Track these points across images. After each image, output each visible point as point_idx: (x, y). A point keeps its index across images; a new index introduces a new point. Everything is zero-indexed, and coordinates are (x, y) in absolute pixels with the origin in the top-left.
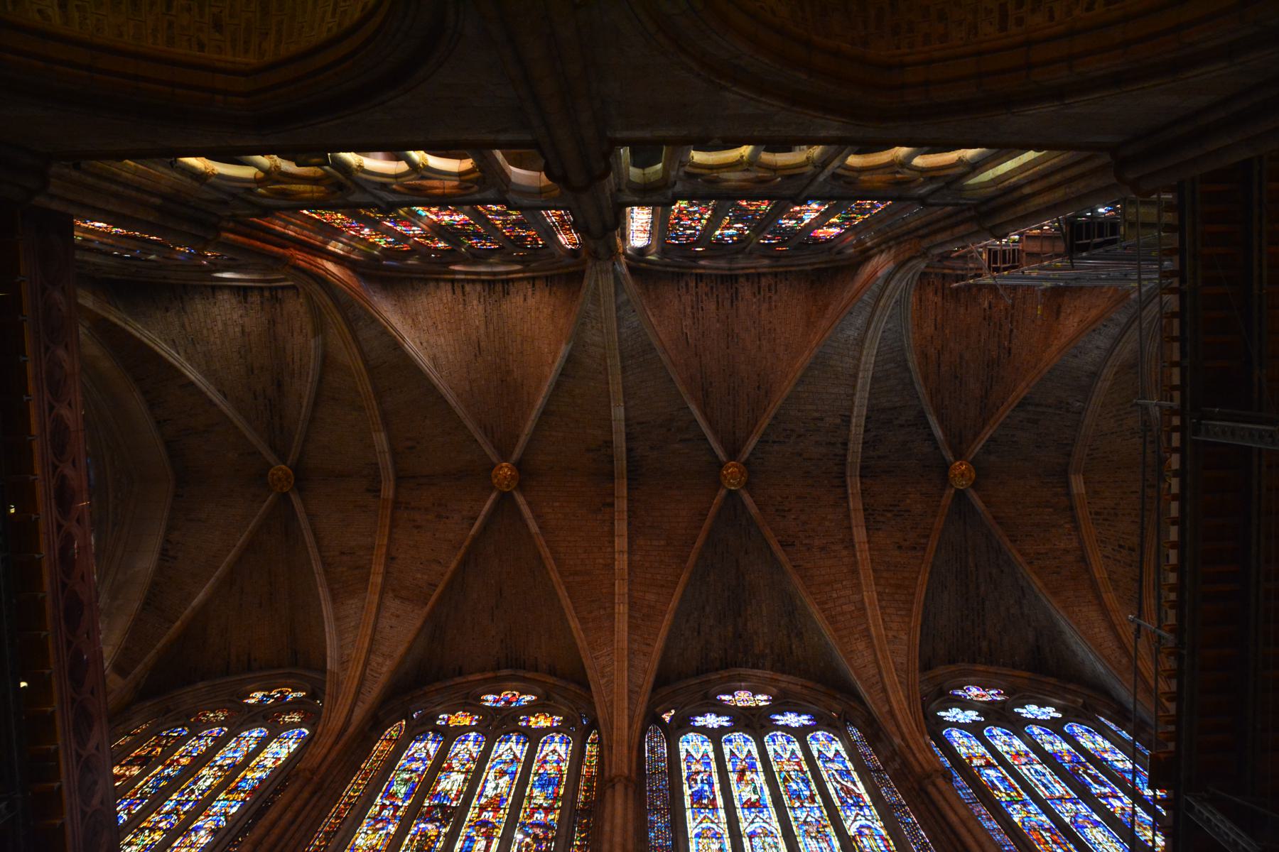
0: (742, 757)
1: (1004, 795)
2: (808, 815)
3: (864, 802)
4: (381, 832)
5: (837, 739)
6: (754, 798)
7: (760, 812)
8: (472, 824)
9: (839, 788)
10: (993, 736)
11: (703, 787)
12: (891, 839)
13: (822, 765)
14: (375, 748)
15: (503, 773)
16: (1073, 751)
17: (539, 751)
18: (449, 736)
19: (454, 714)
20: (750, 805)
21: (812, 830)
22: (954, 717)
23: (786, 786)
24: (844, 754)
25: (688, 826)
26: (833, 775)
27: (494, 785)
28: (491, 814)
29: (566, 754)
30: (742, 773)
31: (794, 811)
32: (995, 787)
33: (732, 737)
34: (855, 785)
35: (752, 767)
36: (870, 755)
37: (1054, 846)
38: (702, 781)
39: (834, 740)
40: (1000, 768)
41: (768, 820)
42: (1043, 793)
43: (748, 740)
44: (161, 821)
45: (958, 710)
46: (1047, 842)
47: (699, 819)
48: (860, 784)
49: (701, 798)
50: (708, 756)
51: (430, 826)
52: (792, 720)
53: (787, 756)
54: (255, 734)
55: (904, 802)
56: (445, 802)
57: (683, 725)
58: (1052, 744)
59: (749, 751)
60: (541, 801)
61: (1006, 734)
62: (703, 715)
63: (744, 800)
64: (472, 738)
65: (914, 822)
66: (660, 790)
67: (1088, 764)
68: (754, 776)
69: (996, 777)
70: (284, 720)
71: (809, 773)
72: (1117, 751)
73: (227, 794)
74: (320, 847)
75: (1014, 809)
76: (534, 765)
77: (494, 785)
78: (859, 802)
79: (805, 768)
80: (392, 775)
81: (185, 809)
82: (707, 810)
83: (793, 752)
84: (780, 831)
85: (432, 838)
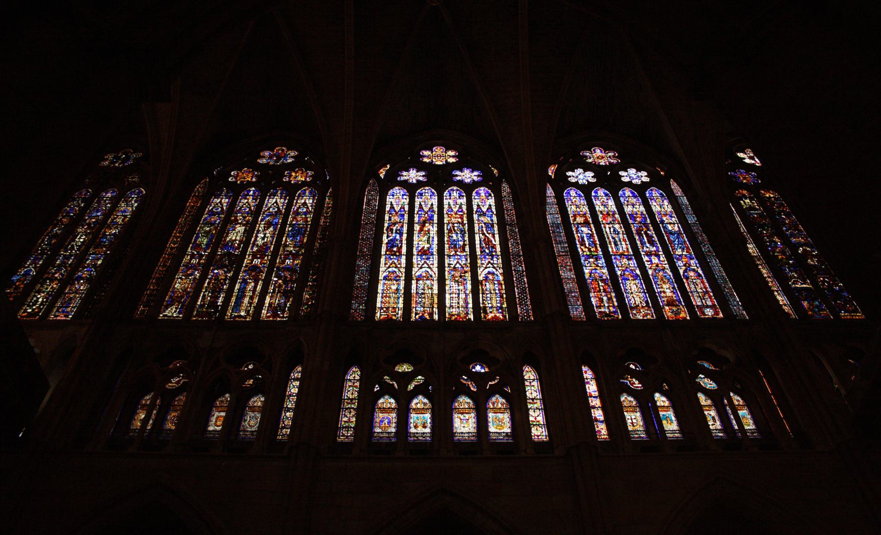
0: (426, 209)
1: (587, 250)
2: (458, 262)
3: (496, 252)
4: (190, 278)
5: (493, 195)
7: (428, 259)
8: (247, 269)
9: (482, 240)
10: (596, 197)
11: (396, 237)
12: (505, 284)
13: (477, 218)
14: (188, 204)
15: (269, 225)
16: (645, 213)
17: (294, 204)
18: (237, 191)
19: (241, 171)
20: (424, 253)
21: (457, 274)
22: (577, 177)
23: (449, 236)
24: (494, 210)
25: (381, 269)
26: (482, 227)
27: (263, 236)
28: (259, 260)
29: (311, 206)
30: (423, 225)
31: (450, 258)
32: (583, 243)
34: (494, 237)
35: (431, 218)
36: (511, 210)
37: (603, 294)
38: (396, 230)
39: (490, 195)
41: (431, 266)
42: (612, 249)
43: (433, 193)
44: (56, 273)
45: (581, 170)
46: (600, 291)
47: (389, 264)
48: (497, 236)
49: (393, 246)
50: (404, 208)
51: (221, 272)
52: (467, 176)
53: (455, 210)
54: (109, 195)
55: (521, 253)
56: (231, 251)
57: (392, 181)
58: (633, 205)
59: (432, 205)
60: (292, 249)
61: (606, 195)
62: (408, 171)
63: (420, 248)
64: (251, 193)
65: (522, 269)
67: (650, 225)
68: (431, 228)
69: (587, 234)
70: (128, 181)
71: (467, 225)
72: (674, 215)
73: (94, 249)
74: (153, 290)
75: (589, 262)
76: (290, 216)
77: (264, 236)
79: (465, 222)
80: (198, 229)
81: (69, 263)
82: (395, 257)
83: (460, 207)
85: (222, 281)
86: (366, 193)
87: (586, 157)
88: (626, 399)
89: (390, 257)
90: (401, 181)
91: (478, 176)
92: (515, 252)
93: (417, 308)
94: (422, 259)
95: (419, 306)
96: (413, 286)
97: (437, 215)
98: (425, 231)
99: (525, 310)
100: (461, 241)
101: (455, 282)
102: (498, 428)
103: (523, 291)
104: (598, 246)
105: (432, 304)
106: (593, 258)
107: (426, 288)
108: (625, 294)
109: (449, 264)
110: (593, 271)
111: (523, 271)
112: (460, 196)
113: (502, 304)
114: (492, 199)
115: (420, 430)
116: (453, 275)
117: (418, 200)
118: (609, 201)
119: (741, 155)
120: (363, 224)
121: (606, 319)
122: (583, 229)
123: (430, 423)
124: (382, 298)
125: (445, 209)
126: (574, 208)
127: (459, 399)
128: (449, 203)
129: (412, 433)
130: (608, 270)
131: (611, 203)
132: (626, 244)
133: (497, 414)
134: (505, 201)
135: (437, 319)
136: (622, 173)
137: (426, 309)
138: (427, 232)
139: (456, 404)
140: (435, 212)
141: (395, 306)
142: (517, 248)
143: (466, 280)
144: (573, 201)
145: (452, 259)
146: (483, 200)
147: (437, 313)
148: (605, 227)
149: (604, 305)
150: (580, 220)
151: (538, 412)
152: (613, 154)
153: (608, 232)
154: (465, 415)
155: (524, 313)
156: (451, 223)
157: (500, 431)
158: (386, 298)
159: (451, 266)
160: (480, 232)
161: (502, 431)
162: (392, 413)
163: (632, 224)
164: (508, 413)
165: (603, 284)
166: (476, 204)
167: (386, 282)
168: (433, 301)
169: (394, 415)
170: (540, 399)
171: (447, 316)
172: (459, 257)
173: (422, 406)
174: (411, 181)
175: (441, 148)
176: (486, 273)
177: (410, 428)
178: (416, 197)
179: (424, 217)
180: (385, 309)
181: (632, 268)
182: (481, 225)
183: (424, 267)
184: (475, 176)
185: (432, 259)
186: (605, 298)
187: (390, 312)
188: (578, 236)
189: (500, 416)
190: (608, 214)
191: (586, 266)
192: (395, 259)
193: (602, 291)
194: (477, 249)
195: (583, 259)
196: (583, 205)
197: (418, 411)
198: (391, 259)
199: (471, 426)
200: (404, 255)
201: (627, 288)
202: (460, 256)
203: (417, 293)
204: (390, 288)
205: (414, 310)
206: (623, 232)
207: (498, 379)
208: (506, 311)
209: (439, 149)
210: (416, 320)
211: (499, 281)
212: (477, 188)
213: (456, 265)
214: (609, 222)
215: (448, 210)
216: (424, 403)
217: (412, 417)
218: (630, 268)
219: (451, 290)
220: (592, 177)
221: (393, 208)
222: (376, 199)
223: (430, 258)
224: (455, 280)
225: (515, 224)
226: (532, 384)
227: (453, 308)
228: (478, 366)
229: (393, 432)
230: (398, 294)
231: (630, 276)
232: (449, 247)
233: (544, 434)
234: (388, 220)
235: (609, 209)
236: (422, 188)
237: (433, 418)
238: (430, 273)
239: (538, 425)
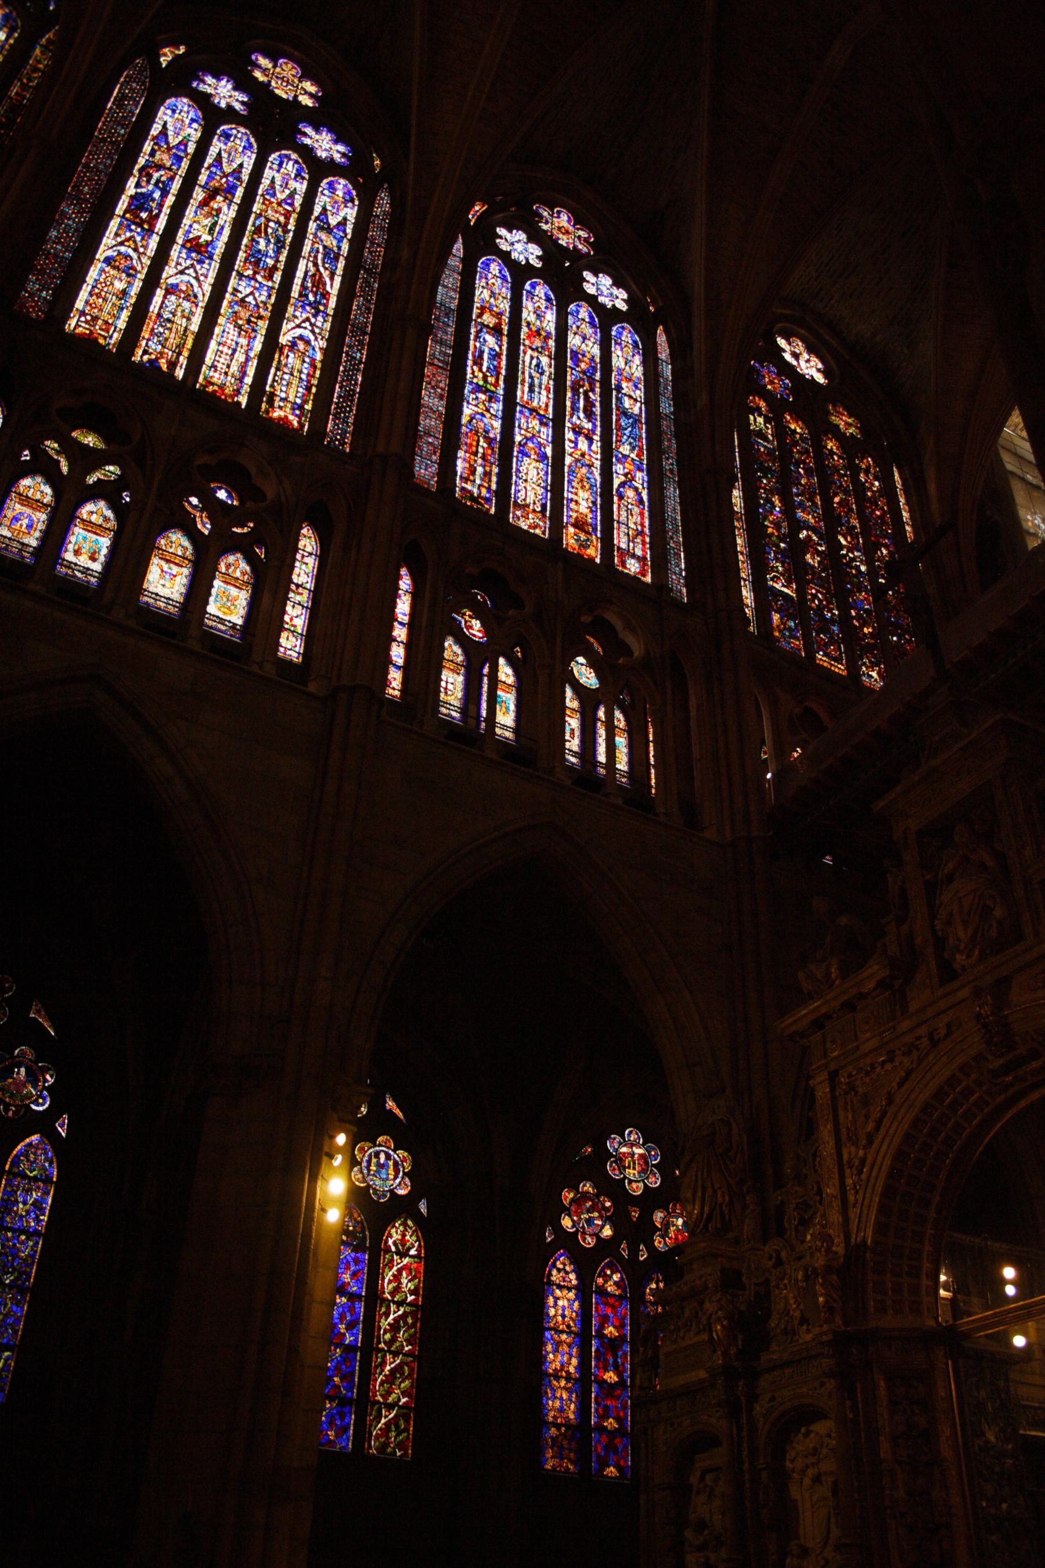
0: (228, 169)
1: (481, 375)
2: (252, 293)
3: (326, 306)
5: (357, 203)
6: (206, 237)
9: (310, 274)
11: (153, 192)
12: (322, 369)
13: (313, 231)
16: (598, 360)
20: (197, 248)
21: (244, 314)
22: (512, 244)
23: (253, 240)
24: (349, 231)
26: (318, 251)
31: (240, 279)
32: (478, 361)
33: (234, 132)
34: (332, 279)
35: (231, 190)
36: (379, 245)
37: (480, 461)
38: (158, 181)
39: (352, 201)
40: (505, 339)
41: (202, 278)
42: (522, 393)
43: (251, 146)
46: (476, 454)
47: (123, 237)
48: (338, 280)
49: (142, 208)
50: (186, 146)
53: (281, 196)
55: (369, 329)
58: (584, 338)
59: (241, 166)
61: (548, 299)
62: (218, 77)
63: (191, 236)
65: (361, 358)
66: (98, 170)
67: (598, 385)
68: (225, 209)
69: (491, 349)
71: (291, 234)
72: (641, 386)
75: (477, 398)
78: (320, 303)
82: (139, 230)
83: (291, 196)
84: (206, 299)
86: (122, 79)
87: (541, 217)
88: (452, 650)
89: (129, 226)
90: (196, 90)
91: (344, 155)
92: (359, 323)
93: (150, 343)
94: (188, 257)
95: (155, 341)
96: (155, 299)
97: (243, 190)
98: (212, 209)
99: (342, 429)
100: (271, 257)
101: (235, 326)
102: (222, 609)
103: (348, 396)
104: (502, 378)
105: (180, 347)
106: (485, 394)
107: (179, 314)
108: (514, 478)
109: (236, 290)
110: (478, 416)
111: (360, 362)
112: (298, 175)
113: (305, 402)
114: (352, 208)
115: (83, 561)
116: (236, 313)
117: (218, 143)
118: (549, 312)
119: (781, 342)
120: (97, 137)
121: (469, 504)
122: (488, 337)
123: (105, 556)
124: (91, 294)
125: (262, 186)
126: (486, 294)
127: (170, 535)
128: (273, 178)
129: (67, 561)
130: (502, 425)
131: (551, 317)
132: (547, 396)
133: (229, 587)
134: (374, 223)
135: (181, 377)
136: (587, 275)
137: (166, 350)
138: (214, 213)
139: (163, 542)
140: (242, 182)
141: (110, 321)
142: (364, 317)
143: (254, 331)
144: (490, 282)
145: (244, 284)
146: (336, 202)
147: (184, 367)
148: (525, 353)
149: (474, 481)
150: (488, 319)
151: (298, 610)
152: (586, 236)
153: (527, 364)
154: (172, 565)
155: (338, 434)
156: (265, 217)
157: (224, 617)
158: (98, 298)
159: (239, 294)
160: (311, 259)
161: (228, 618)
162: (40, 511)
163: (570, 367)
164: (248, 591)
165: (485, 445)
166: (322, 204)
167: (107, 269)
168: (184, 343)
169: (43, 517)
170: (310, 590)
171: (201, 379)
172: (257, 285)
173: (100, 521)
174: (216, 101)
175: (293, 68)
176: (296, 335)
177: (66, 551)
178: (216, 137)
179: (219, 182)
180: (89, 318)
181: (542, 441)
182: (316, 245)
183: (189, 275)
184: (338, 151)
185: (208, 267)
186: (480, 470)
187: (97, 327)
188: (475, 346)
189: (233, 591)
190: (538, 333)
191: (468, 403)
192: (138, 233)
193: (480, 455)
194: (294, 286)
195: (468, 388)
196: (503, 298)
197: (89, 526)
198: (131, 231)
199: (176, 588)
200: (157, 233)
201: (521, 469)
202: (260, 283)
203: (159, 315)
204: (112, 284)
205: (144, 343)
206: (551, 374)
207: (249, 527)
208: (306, 417)
209: (290, 66)
210: (141, 363)
211: (313, 360)
212: (334, 176)
213: (247, 296)
214: (534, 347)
215: (267, 190)
216: (105, 517)
217: (76, 533)
218: (539, 439)
219: (222, 337)
220: (538, 257)
221: (166, 136)
222: (138, 102)
223: (204, 262)
224: (236, 323)
225: (375, 273)
226: (306, 560)
227: (215, 371)
228: (223, 491)
229: (31, 546)
230: (123, 302)
231: (533, 452)
232: (246, 259)
233: (297, 649)
234: (148, 152)
235: (544, 325)
236: (234, 126)
237: (113, 550)
238: (196, 291)
239: (293, 632)
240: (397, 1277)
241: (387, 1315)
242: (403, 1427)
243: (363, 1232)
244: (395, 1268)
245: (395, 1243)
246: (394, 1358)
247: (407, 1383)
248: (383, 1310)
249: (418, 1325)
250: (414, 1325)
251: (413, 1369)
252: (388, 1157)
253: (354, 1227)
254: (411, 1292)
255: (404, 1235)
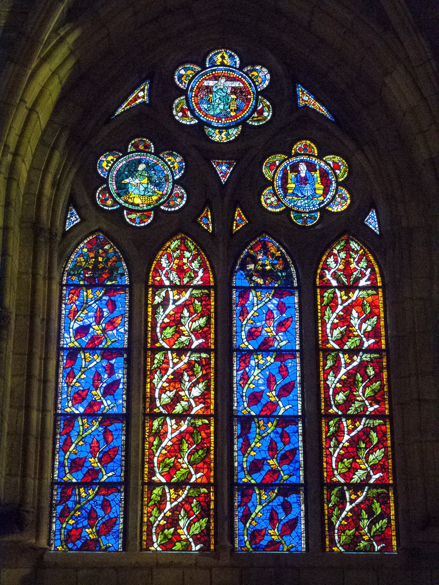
240: (345, 319)
241: (336, 368)
242: (379, 511)
243: (286, 268)
244: (340, 308)
245: (334, 275)
246: (353, 423)
247: (379, 454)
248: (330, 363)
249: (385, 375)
250: (378, 377)
251: (385, 434)
252: (311, 167)
253: (273, 265)
254: (368, 335)
255: (347, 264)
